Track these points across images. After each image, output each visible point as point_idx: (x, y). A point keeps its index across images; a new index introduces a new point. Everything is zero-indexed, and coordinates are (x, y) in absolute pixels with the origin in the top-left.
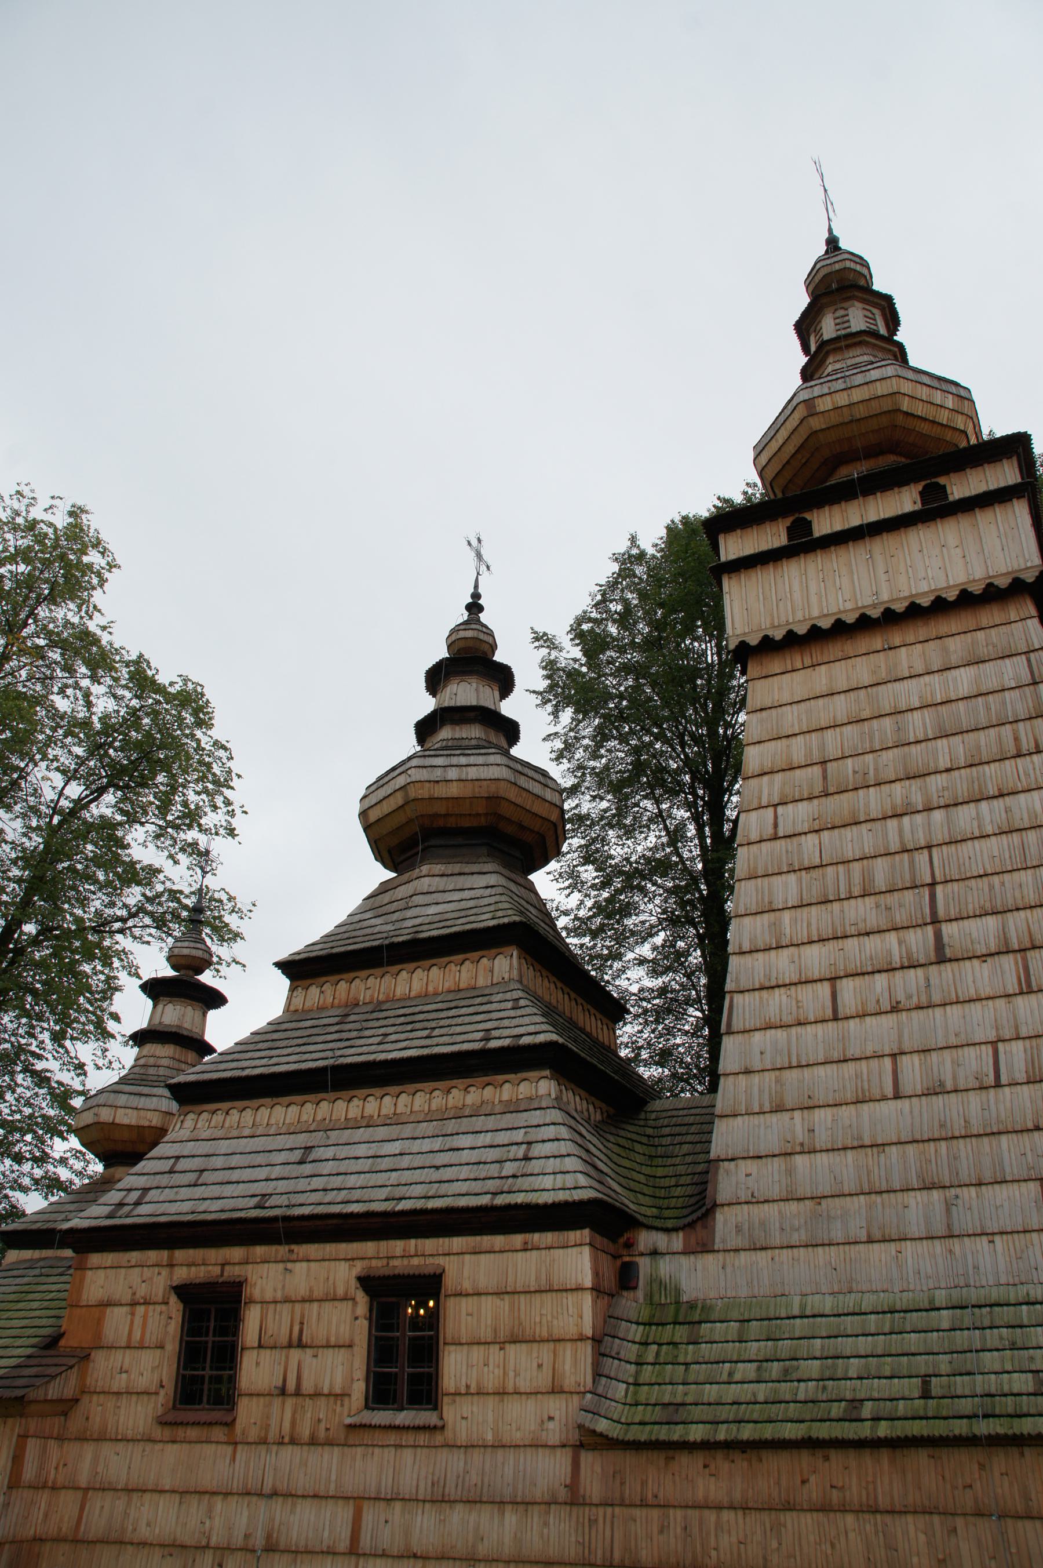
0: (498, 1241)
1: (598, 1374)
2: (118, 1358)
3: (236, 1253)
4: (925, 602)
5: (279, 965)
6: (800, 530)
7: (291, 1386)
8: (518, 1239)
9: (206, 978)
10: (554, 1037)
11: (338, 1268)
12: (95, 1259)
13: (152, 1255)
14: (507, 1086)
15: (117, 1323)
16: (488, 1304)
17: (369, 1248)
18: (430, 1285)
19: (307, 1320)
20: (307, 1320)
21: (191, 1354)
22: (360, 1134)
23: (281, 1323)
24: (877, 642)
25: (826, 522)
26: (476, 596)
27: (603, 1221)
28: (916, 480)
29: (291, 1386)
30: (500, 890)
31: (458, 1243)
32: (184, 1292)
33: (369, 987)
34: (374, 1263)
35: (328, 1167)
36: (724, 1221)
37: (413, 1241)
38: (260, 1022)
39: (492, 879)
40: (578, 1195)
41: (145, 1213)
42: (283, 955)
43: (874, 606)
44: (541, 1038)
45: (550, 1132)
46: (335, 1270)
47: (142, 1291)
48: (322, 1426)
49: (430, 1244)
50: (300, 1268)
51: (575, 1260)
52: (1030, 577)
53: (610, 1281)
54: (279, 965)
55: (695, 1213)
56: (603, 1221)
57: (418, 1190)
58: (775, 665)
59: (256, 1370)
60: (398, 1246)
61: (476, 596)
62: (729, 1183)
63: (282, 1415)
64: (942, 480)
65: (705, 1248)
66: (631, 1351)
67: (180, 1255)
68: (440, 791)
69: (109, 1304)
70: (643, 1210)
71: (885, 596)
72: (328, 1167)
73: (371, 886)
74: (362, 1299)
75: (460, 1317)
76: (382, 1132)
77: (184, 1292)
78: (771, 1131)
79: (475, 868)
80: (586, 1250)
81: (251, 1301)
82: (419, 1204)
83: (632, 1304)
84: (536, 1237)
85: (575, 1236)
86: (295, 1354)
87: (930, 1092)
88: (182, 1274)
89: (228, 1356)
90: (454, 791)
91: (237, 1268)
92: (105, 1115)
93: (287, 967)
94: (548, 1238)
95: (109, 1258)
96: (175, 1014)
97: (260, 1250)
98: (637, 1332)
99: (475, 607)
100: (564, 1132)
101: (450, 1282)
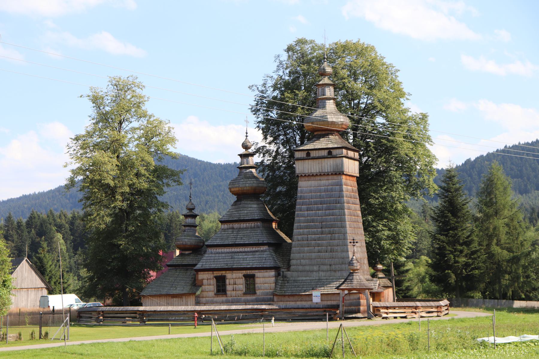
0: (262, 271)
1: (276, 287)
2: (206, 287)
3: (224, 272)
6: (308, 154)
11: (240, 274)
12: (199, 273)
13: (210, 272)
15: (205, 282)
16: (261, 279)
17: (244, 272)
18: (253, 277)
19: (235, 281)
20: (235, 281)
21: (218, 286)
22: (240, 254)
23: (232, 281)
24: (319, 178)
26: (247, 133)
31: (257, 271)
32: (216, 277)
33: (236, 225)
35: (236, 259)
36: (292, 268)
39: (255, 206)
41: (207, 266)
46: (240, 274)
47: (209, 278)
49: (253, 271)
50: (234, 274)
51: (272, 273)
53: (277, 275)
55: (288, 268)
56: (277, 269)
57: (251, 264)
58: (303, 179)
59: (229, 288)
61: (247, 133)
62: (293, 262)
63: (234, 293)
65: (289, 271)
66: (280, 284)
67: (214, 272)
68: (245, 189)
69: (202, 280)
72: (236, 259)
75: (257, 280)
76: (244, 254)
77: (216, 277)
78: (297, 256)
79: (252, 202)
83: (280, 278)
86: (235, 286)
87: (318, 252)
88: (215, 275)
89: (224, 285)
90: (248, 188)
92: (184, 243)
95: (202, 273)
96: (189, 220)
97: (228, 272)
98: (280, 282)
101: (256, 276)
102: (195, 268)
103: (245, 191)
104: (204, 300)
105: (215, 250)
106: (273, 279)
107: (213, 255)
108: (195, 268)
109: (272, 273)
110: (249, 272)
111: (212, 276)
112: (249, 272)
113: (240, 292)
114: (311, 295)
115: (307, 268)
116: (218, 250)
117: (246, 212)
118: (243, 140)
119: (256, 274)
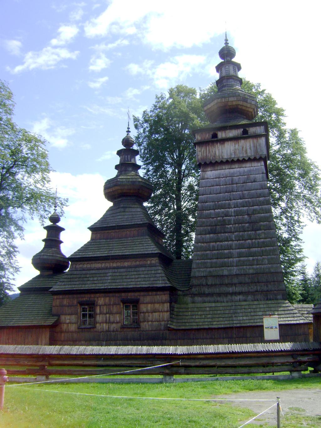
1: (171, 318)
3: (92, 296)
4: (241, 159)
5: (89, 228)
6: (215, 136)
7: (108, 321)
8: (154, 293)
9: (59, 224)
10: (159, 252)
14: (149, 261)
25: (221, 135)
26: (128, 128)
27: (172, 290)
28: (242, 128)
29: (108, 321)
30: (142, 213)
31: (142, 293)
34: (124, 297)
37: (132, 293)
38: (86, 242)
40: (167, 285)
42: (90, 225)
43: (230, 158)
44: (156, 252)
45: (160, 271)
48: (115, 328)
51: (165, 297)
52: (263, 157)
54: (89, 228)
56: (172, 290)
60: (130, 294)
61: (128, 128)
64: (247, 129)
70: (177, 286)
71: (233, 156)
73: (107, 208)
74: (121, 304)
75: (143, 308)
80: (168, 295)
81: (97, 305)
82: (135, 286)
84: (158, 293)
85: (165, 292)
91: (93, 299)
93: (91, 228)
94: (161, 293)
99: (128, 131)
100: (162, 272)
101: (141, 301)
102: (51, 290)
103: (125, 191)
104: (63, 336)
105: (81, 266)
106: (167, 306)
107: (78, 272)
108: (51, 290)
109: (165, 297)
110: (131, 296)
111: (75, 302)
112: (131, 296)
113: (114, 325)
114: (262, 326)
115: (217, 290)
116: (85, 266)
117: (126, 217)
118: (124, 135)
119: (142, 299)
